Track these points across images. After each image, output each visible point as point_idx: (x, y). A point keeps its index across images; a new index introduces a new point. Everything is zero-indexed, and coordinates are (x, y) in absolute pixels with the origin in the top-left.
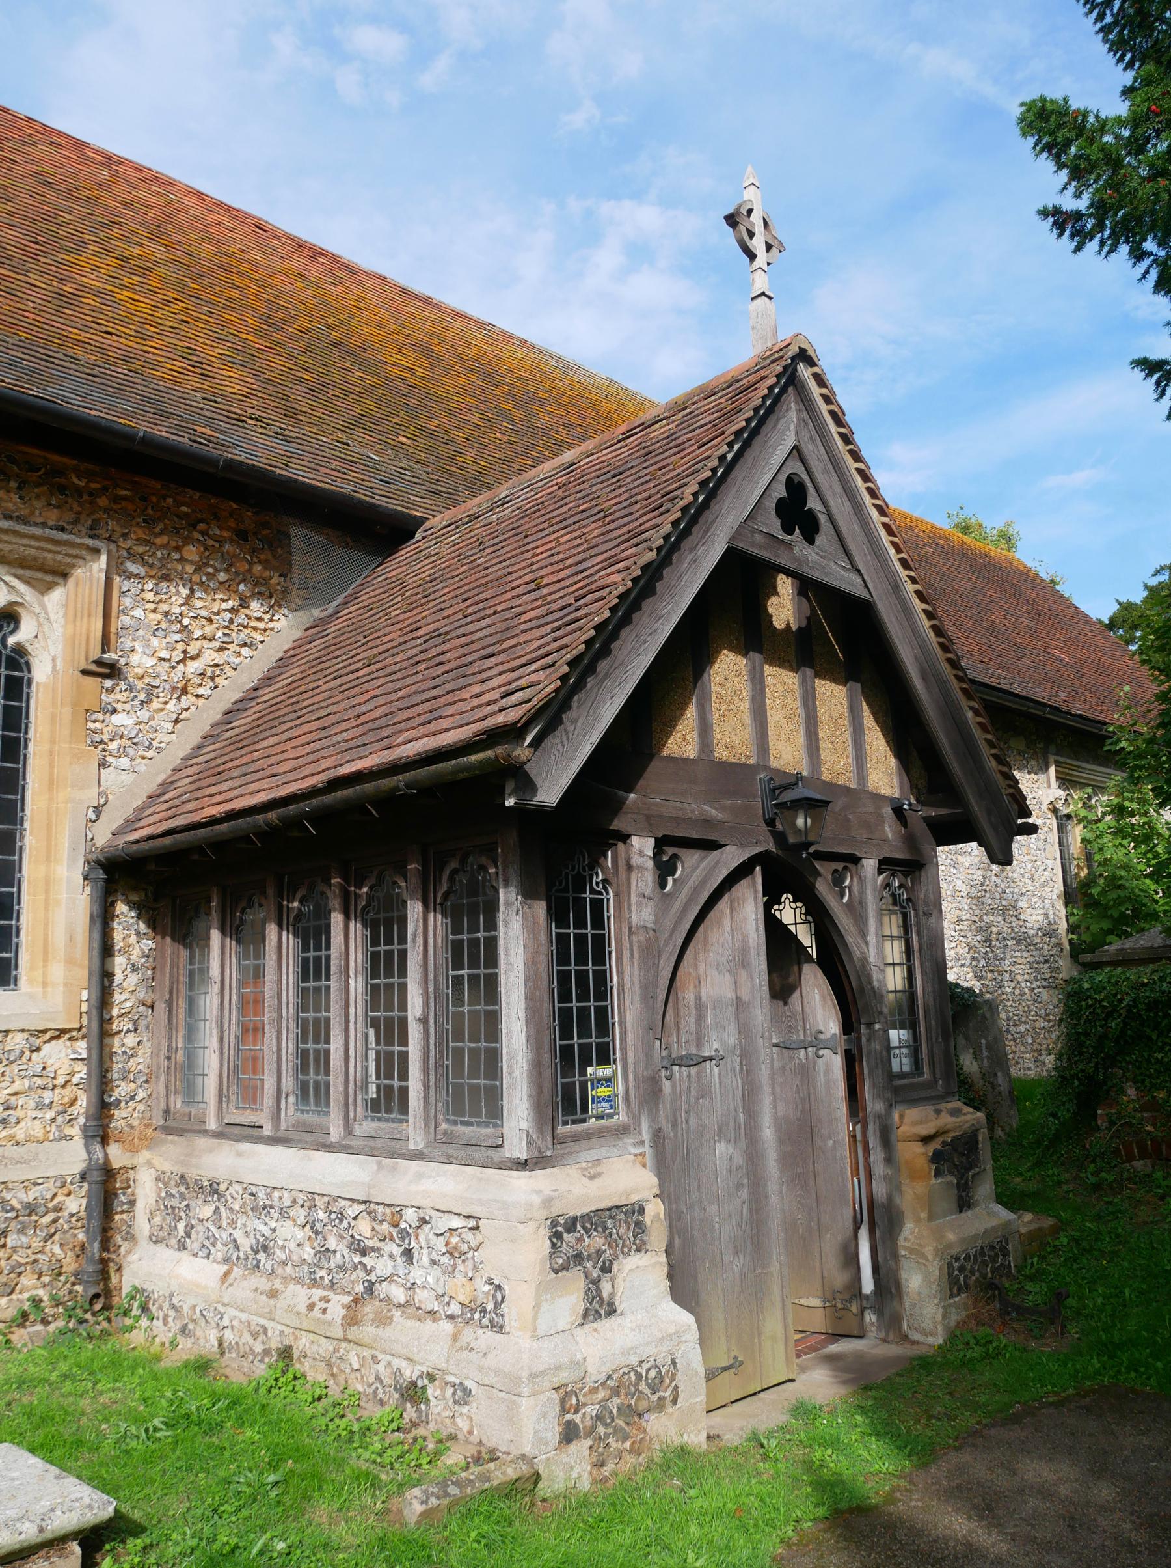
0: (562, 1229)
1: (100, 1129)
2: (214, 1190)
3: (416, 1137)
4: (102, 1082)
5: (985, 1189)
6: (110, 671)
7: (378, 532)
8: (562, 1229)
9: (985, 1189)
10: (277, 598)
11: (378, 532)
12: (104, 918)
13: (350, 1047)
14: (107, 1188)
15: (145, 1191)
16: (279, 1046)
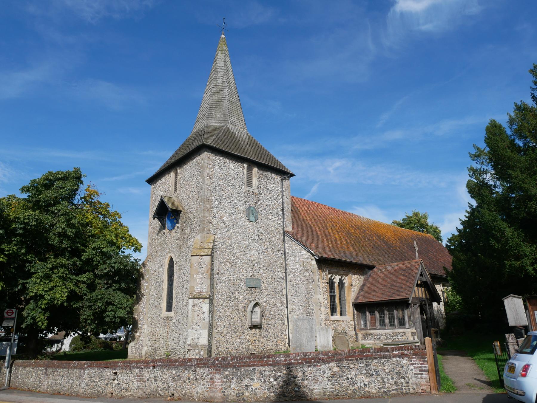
0: (412, 333)
1: (355, 330)
2: (371, 334)
3: (397, 328)
4: (355, 325)
5: (439, 336)
6: (352, 285)
7: (371, 268)
8: (412, 333)
9: (439, 336)
10: (361, 275)
11: (371, 268)
12: (353, 310)
13: (387, 321)
14: (356, 334)
15: (360, 336)
16: (378, 321)
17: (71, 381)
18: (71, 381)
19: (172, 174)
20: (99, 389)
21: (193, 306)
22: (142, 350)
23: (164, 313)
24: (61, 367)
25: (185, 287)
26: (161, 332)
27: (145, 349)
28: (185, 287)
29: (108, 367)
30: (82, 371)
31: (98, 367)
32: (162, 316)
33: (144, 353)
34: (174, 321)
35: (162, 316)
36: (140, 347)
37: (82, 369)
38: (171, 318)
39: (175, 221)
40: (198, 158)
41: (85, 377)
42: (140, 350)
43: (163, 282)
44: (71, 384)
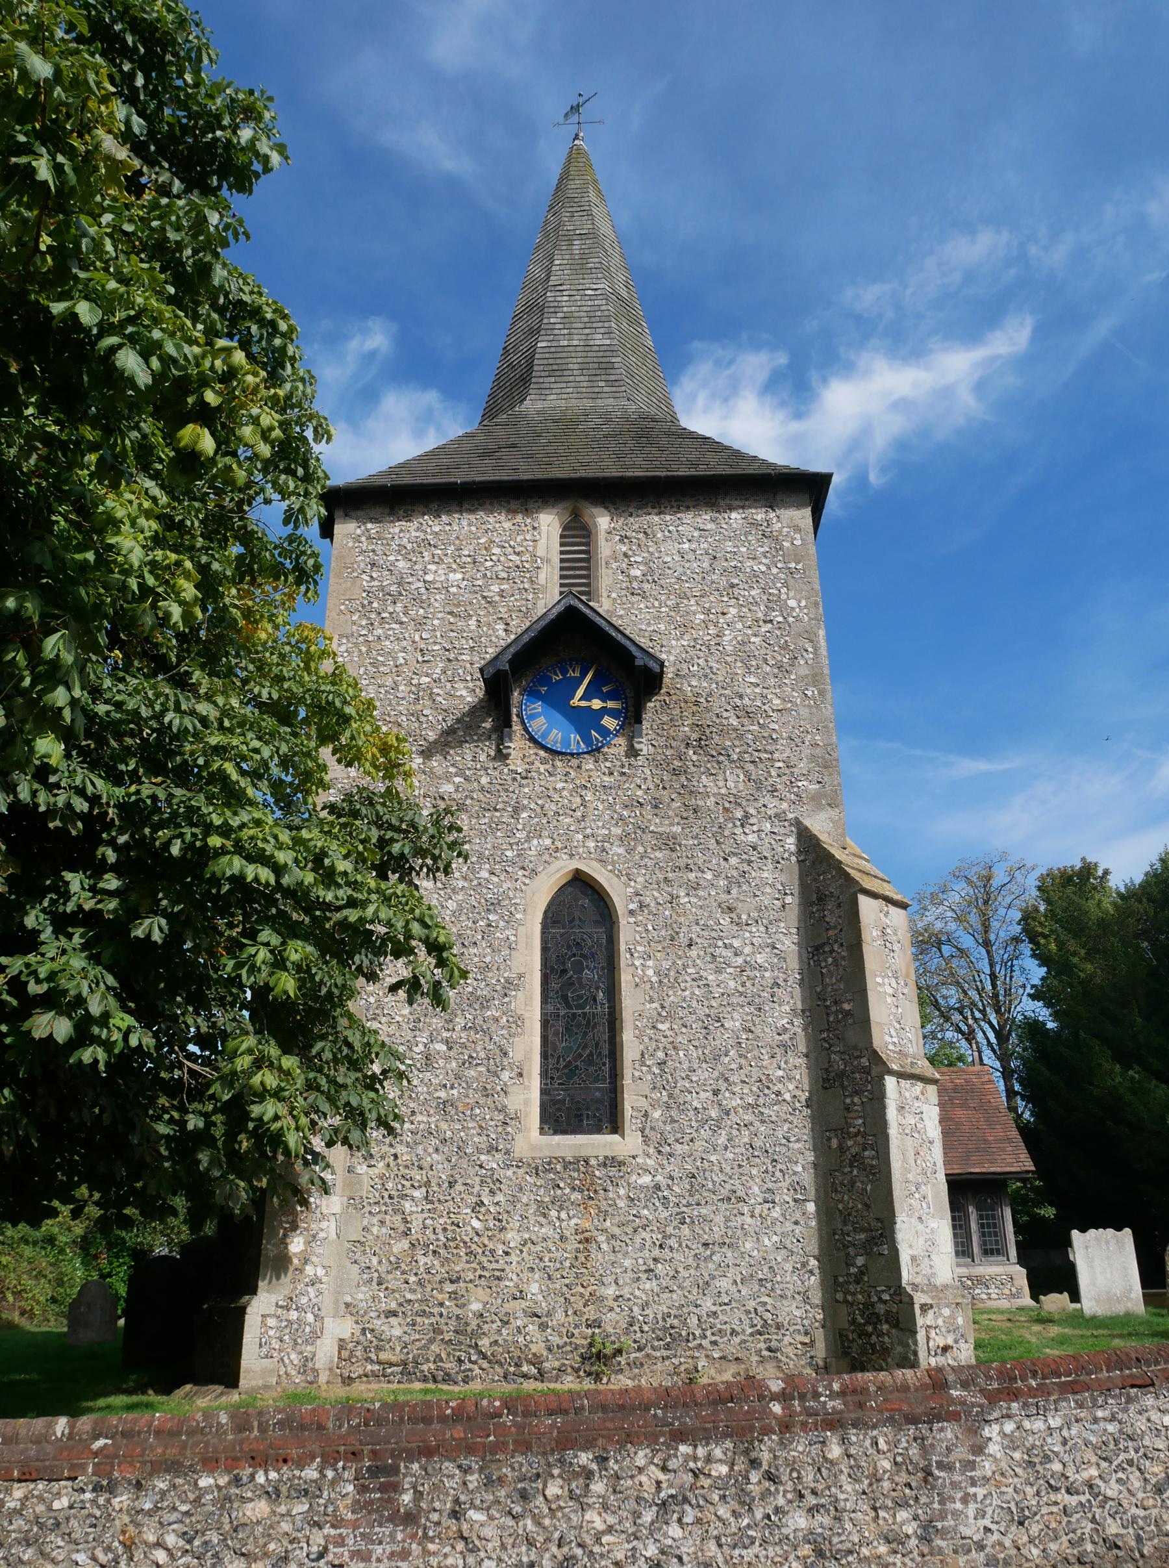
17: (798, 1521)
18: (798, 1521)
19: (548, 524)
20: (1113, 1528)
21: (901, 1108)
22: (316, 1336)
23: (532, 1138)
24: (629, 1439)
25: (734, 1023)
26: (513, 1237)
27: (340, 1328)
28: (734, 1023)
29: (1145, 1385)
30: (948, 1432)
31: (1073, 1388)
32: (521, 1148)
33: (325, 1352)
34: (646, 1180)
35: (521, 1148)
36: (304, 1324)
37: (935, 1417)
38: (611, 1162)
39: (609, 722)
40: (760, 515)
41: (988, 1468)
42: (302, 1336)
43: (510, 986)
44: (810, 1537)
